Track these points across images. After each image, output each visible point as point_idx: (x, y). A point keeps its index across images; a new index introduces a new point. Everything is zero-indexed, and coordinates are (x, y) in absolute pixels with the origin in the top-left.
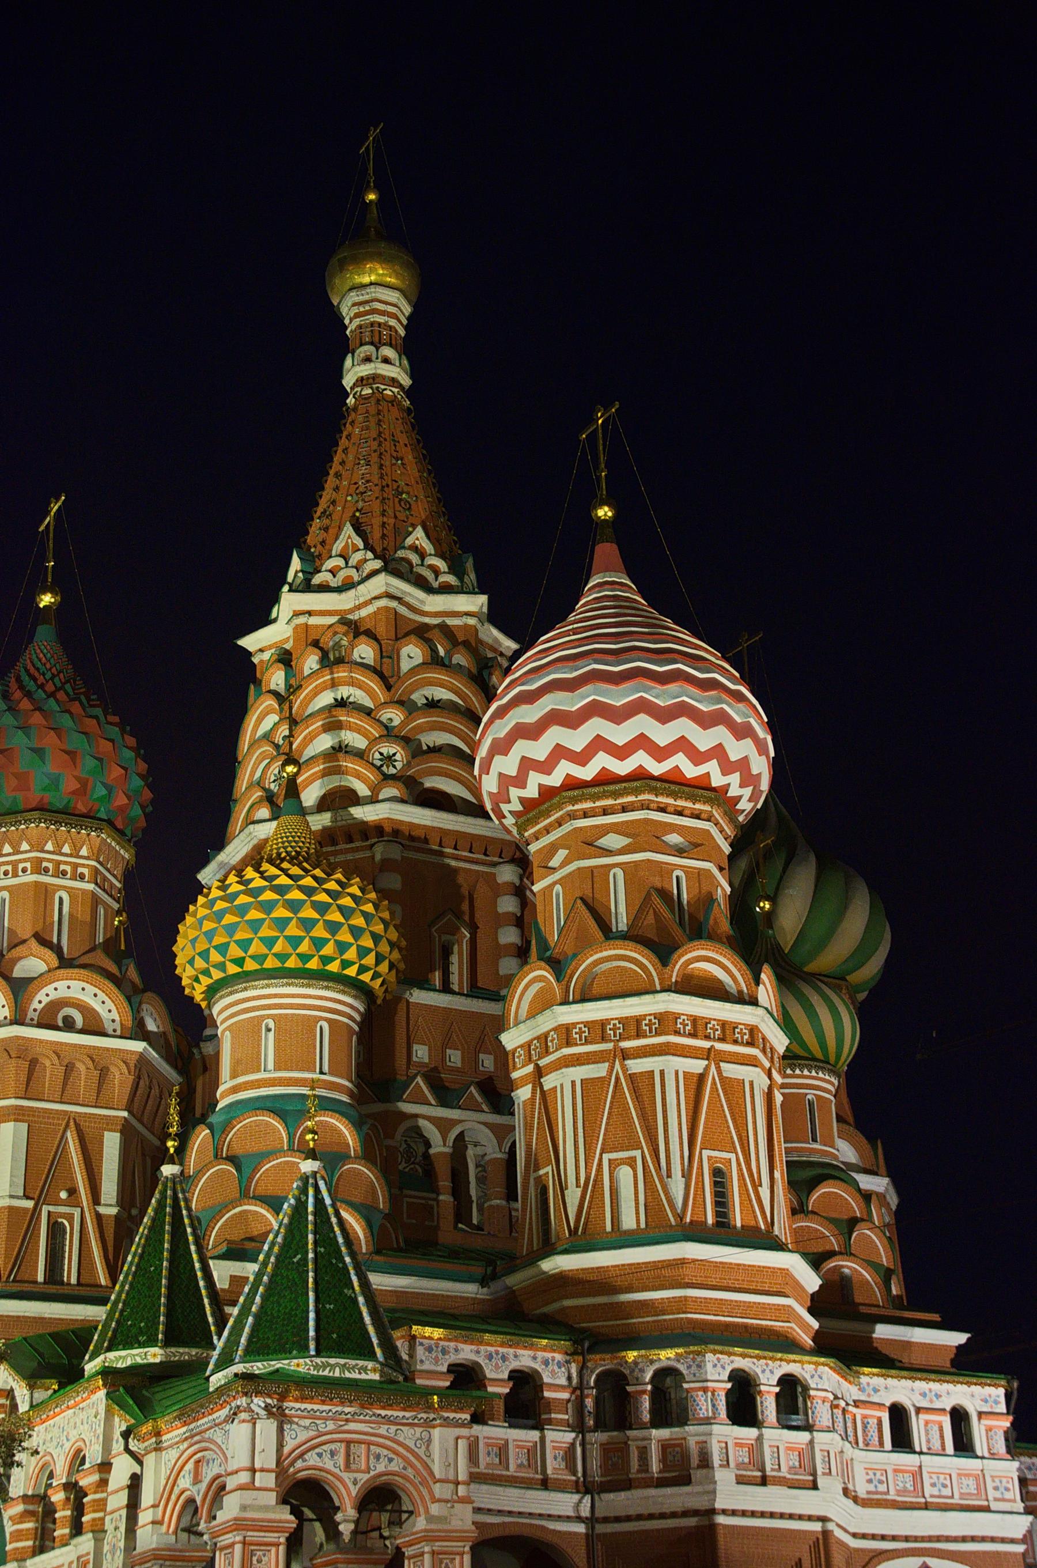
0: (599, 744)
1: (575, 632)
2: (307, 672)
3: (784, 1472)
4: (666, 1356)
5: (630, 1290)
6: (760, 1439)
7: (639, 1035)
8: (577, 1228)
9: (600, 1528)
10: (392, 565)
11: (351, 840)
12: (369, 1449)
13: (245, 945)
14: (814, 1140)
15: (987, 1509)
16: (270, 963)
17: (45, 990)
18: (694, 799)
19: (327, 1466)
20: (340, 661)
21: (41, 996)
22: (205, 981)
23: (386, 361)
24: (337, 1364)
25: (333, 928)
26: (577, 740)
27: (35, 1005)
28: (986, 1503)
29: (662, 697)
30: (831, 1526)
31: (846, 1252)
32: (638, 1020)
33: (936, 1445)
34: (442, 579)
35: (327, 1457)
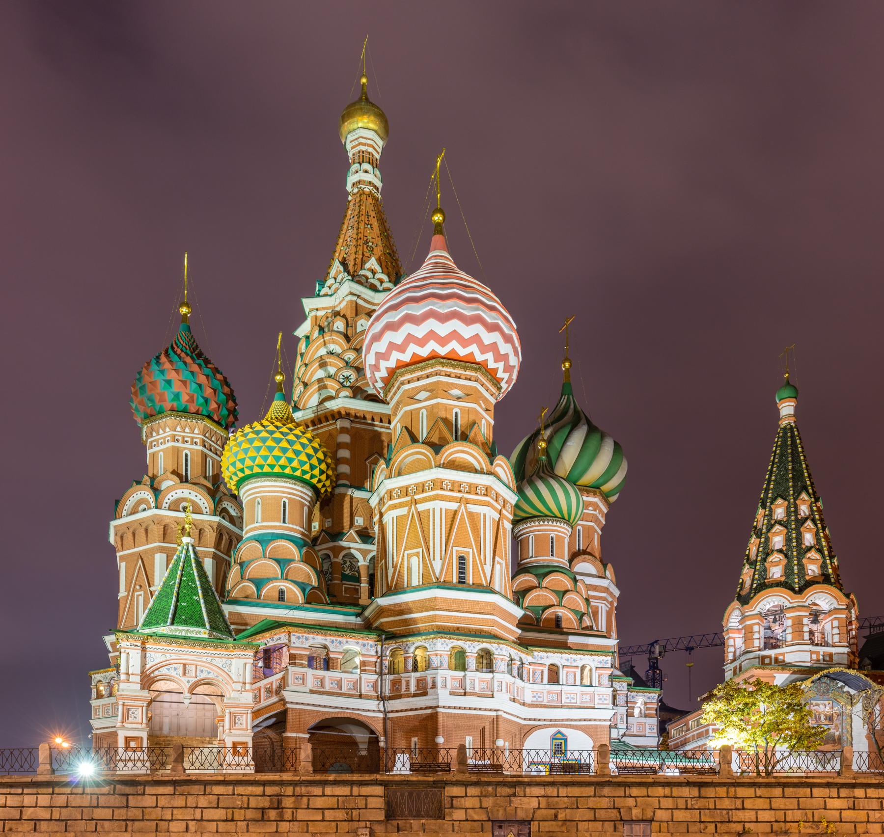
5: (411, 613)
8: (391, 587)
11: (327, 420)
12: (196, 668)
17: (171, 494)
19: (172, 674)
21: (169, 496)
24: (184, 630)
27: (166, 500)
35: (172, 671)
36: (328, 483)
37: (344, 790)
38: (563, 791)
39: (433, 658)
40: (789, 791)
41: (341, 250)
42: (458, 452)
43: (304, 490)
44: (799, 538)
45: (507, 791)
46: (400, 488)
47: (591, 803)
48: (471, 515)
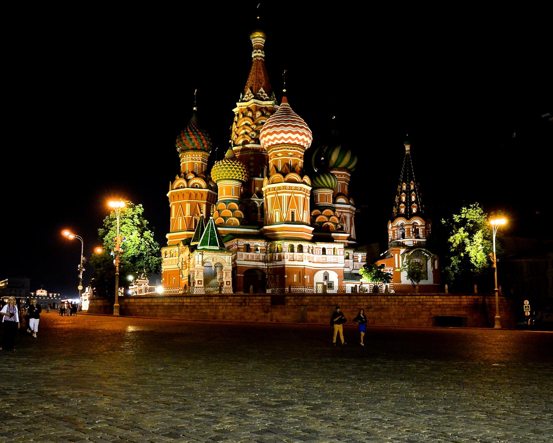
0: (275, 138)
1: (274, 116)
2: (241, 118)
3: (297, 259)
4: (279, 242)
5: (276, 232)
6: (294, 254)
7: (280, 190)
9: (269, 267)
10: (256, 96)
13: (219, 175)
14: (326, 202)
16: (224, 178)
18: (293, 146)
20: (246, 116)
21: (191, 182)
22: (216, 179)
23: (259, 52)
25: (233, 171)
26: (272, 137)
27: (190, 184)
28: (337, 262)
29: (286, 129)
30: (305, 267)
31: (328, 221)
32: (280, 187)
33: (330, 254)
34: (266, 98)
35: (210, 260)
37: (261, 298)
38: (315, 298)
39: (283, 248)
40: (372, 297)
41: (249, 82)
42: (291, 176)
43: (239, 183)
44: (410, 198)
45: (302, 297)
47: (322, 300)
48: (295, 197)
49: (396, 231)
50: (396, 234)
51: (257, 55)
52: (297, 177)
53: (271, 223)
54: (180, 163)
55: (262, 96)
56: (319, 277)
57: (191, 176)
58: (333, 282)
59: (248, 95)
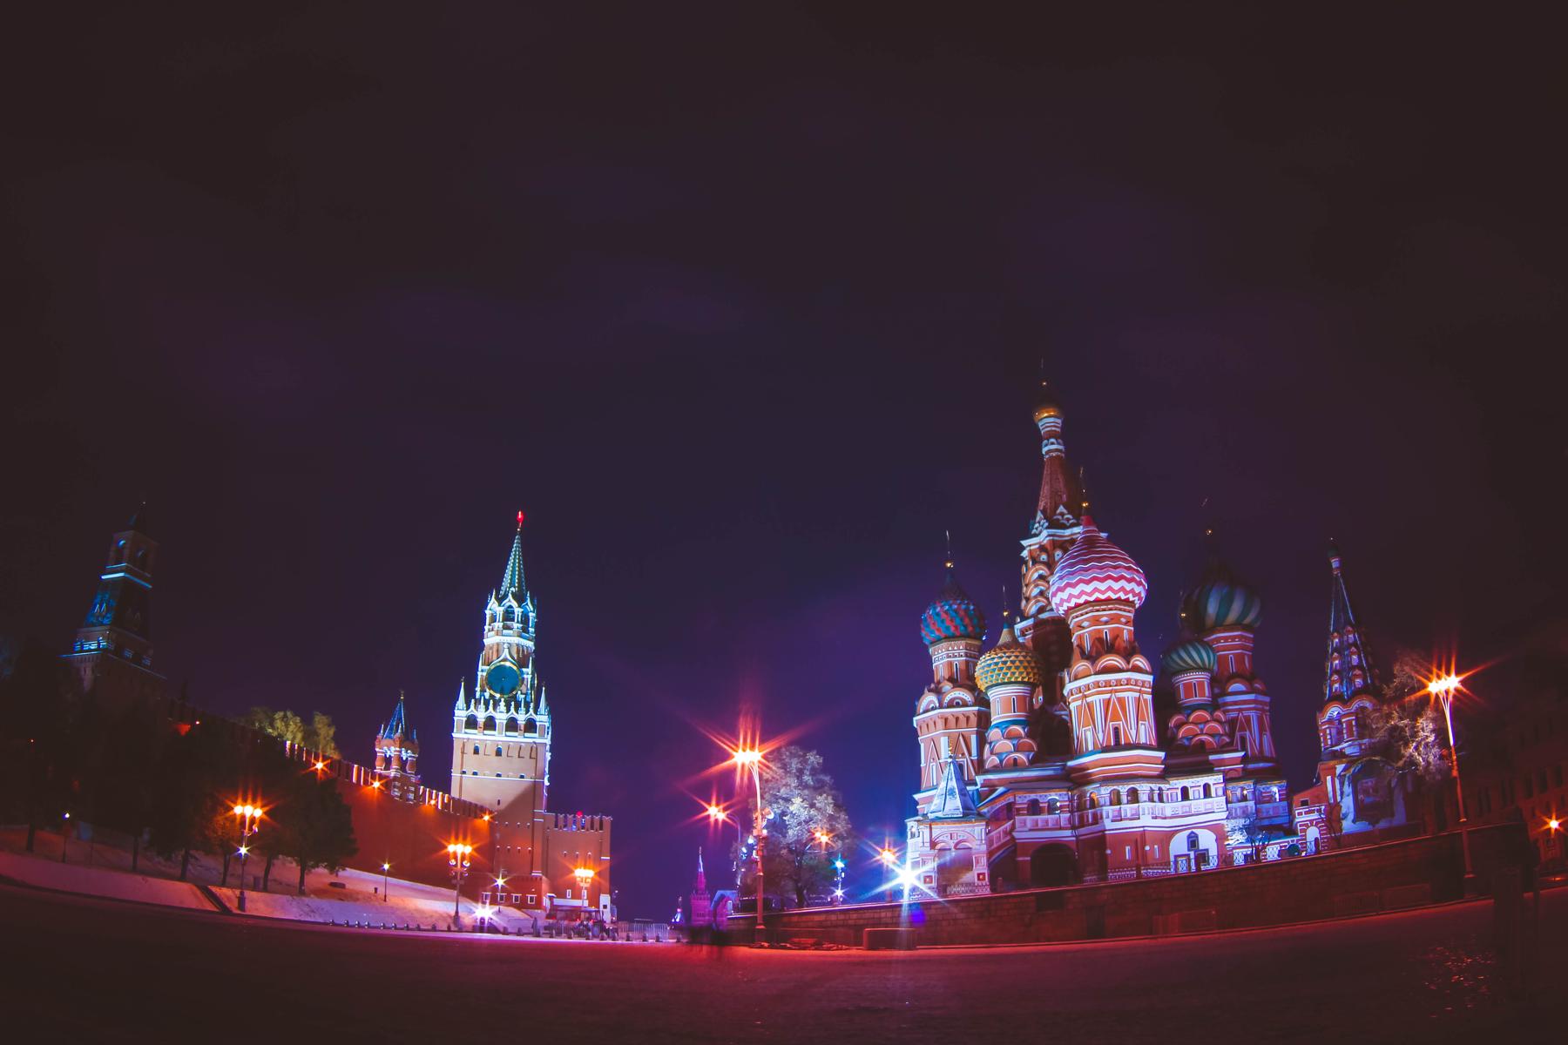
0: (1071, 596)
3: (1129, 816)
7: (1089, 689)
9: (1081, 838)
15: (1213, 812)
23: (1053, 443)
31: (1202, 734)
33: (1197, 796)
34: (1071, 522)
36: (1041, 678)
46: (1076, 688)
49: (1328, 731)
50: (1328, 737)
51: (1050, 448)
52: (1120, 661)
53: (1081, 755)
54: (932, 664)
55: (1062, 521)
56: (1179, 845)
57: (947, 686)
58: (1207, 850)
59: (1039, 522)
